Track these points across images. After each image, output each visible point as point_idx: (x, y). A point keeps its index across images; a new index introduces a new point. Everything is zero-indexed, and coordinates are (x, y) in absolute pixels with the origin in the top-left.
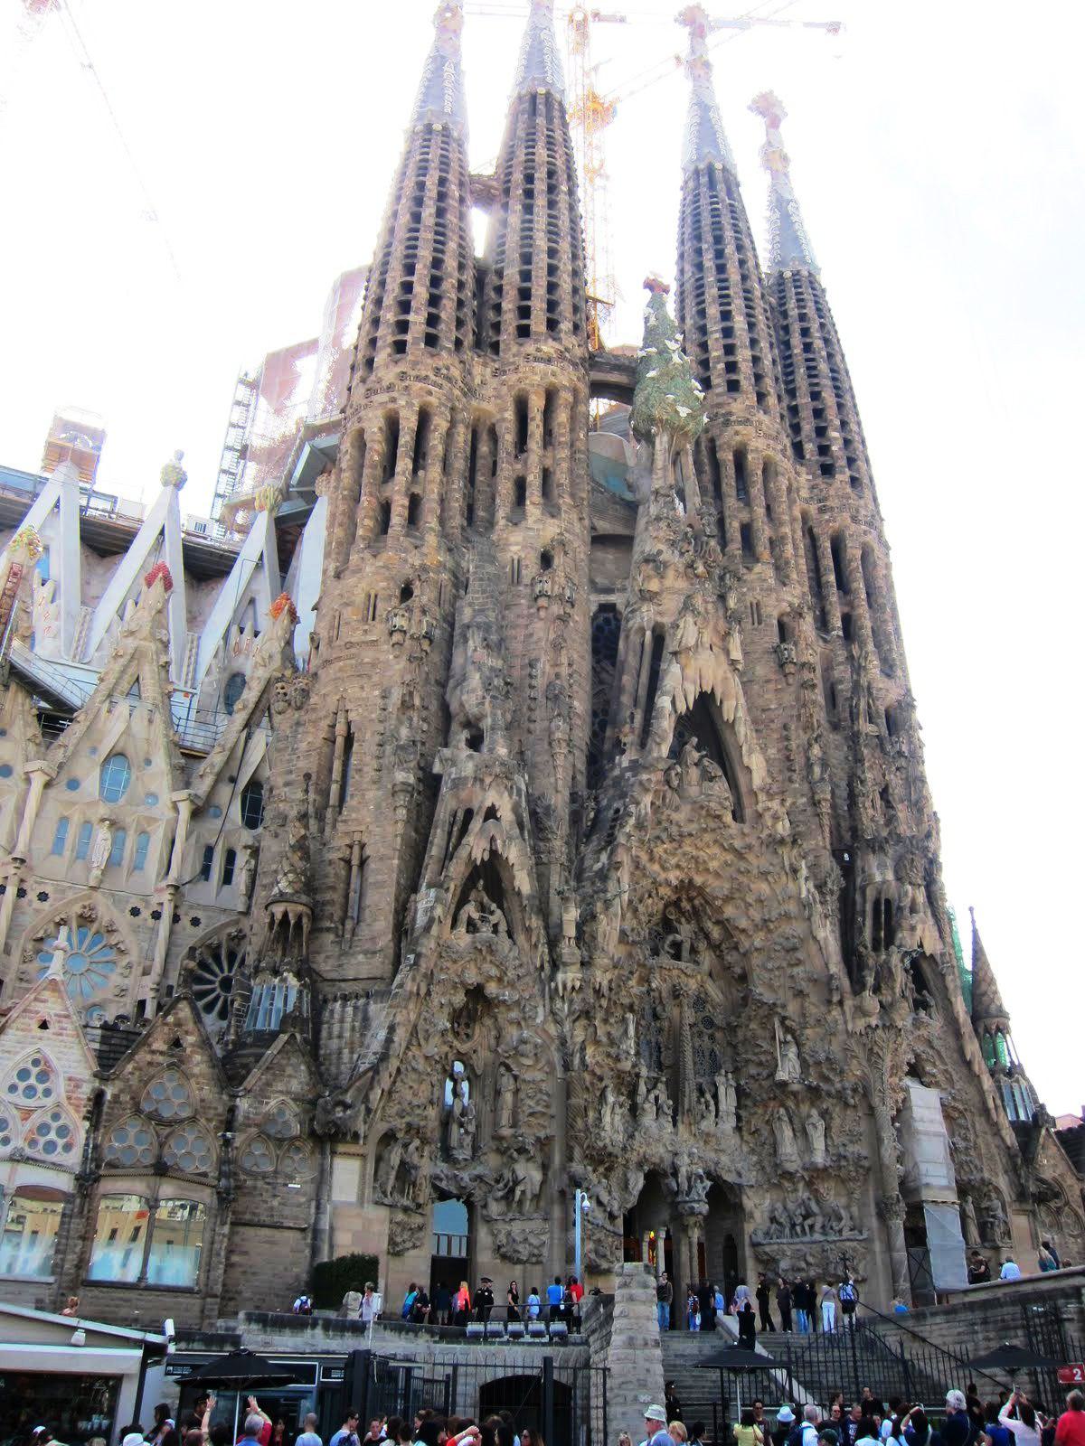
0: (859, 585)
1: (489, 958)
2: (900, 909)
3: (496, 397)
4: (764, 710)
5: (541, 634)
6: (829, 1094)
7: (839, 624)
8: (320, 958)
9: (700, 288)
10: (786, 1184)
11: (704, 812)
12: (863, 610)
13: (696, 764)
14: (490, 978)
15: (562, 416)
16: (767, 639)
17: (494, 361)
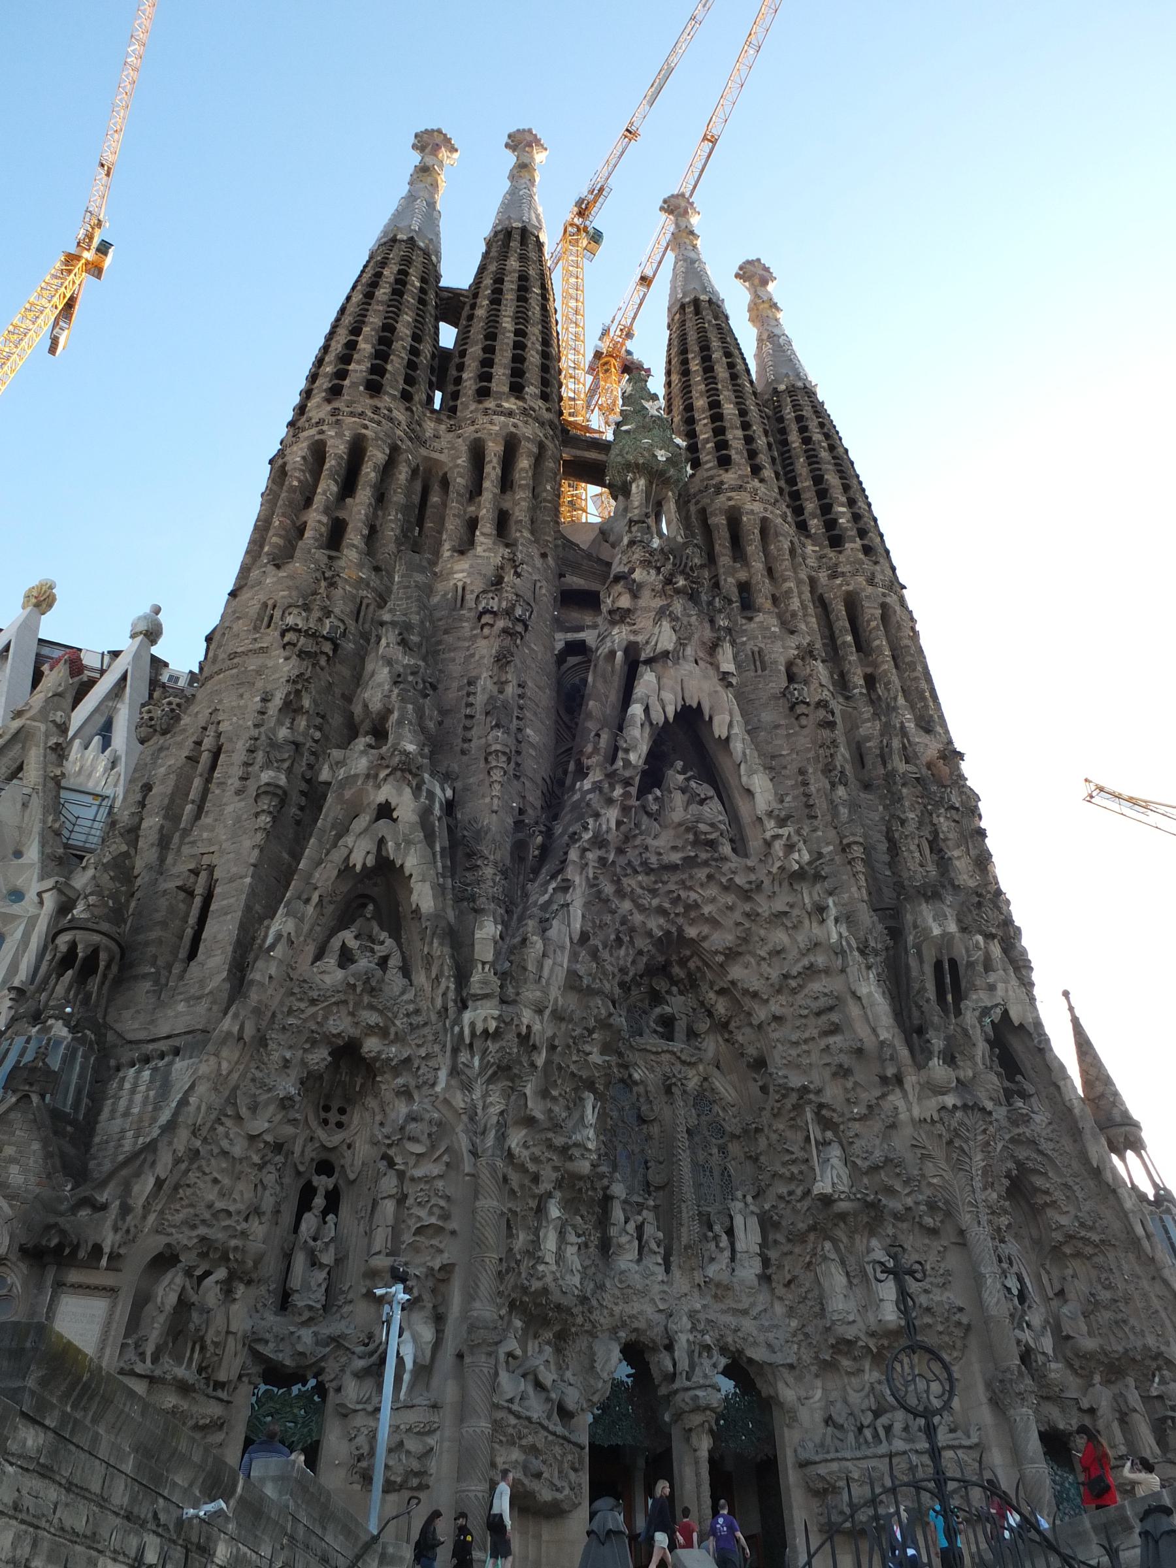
0: (881, 642)
1: (366, 999)
2: (971, 965)
3: (453, 448)
4: (773, 757)
5: (484, 652)
6: (897, 1217)
7: (862, 682)
8: (127, 1014)
9: (686, 389)
10: (846, 1363)
11: (691, 837)
12: (887, 665)
13: (684, 791)
14: (371, 1030)
15: (524, 463)
16: (773, 685)
17: (449, 417)
